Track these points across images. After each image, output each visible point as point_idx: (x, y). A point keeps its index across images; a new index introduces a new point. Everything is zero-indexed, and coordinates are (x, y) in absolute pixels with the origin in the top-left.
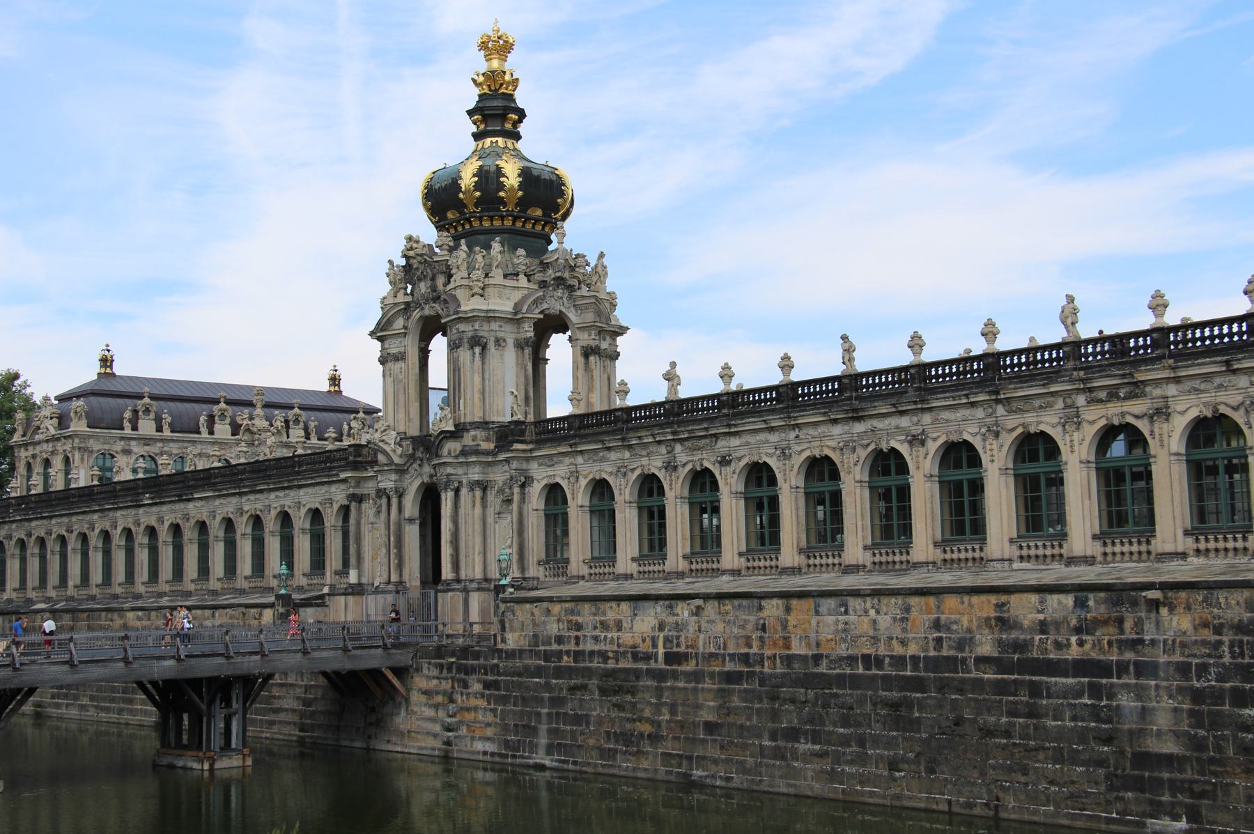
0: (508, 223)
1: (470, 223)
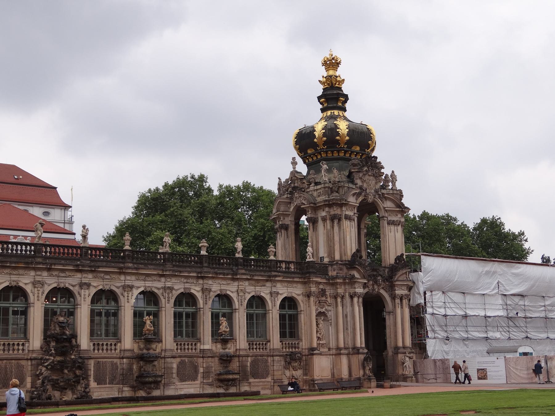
0: (342, 154)
1: (321, 155)
